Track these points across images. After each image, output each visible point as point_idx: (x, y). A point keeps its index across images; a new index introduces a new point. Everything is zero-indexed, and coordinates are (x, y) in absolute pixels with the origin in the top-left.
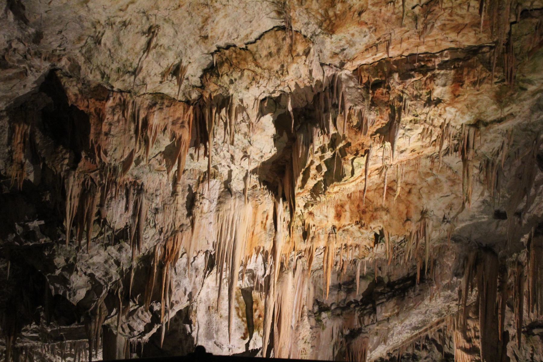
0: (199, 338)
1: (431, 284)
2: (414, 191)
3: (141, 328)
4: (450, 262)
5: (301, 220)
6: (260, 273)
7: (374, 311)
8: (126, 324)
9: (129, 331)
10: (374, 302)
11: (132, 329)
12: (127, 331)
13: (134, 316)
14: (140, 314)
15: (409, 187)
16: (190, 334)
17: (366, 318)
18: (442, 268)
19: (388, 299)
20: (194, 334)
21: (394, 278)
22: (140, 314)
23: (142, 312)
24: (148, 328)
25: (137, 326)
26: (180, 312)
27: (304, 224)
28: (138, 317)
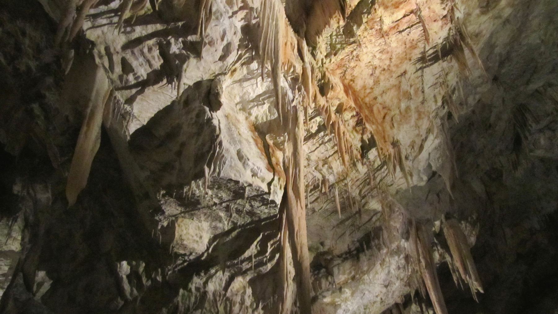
0: (222, 131)
1: (379, 249)
2: (388, 118)
3: (143, 72)
4: (397, 223)
5: (321, 72)
6: (290, 95)
7: (330, 273)
8: (120, 57)
9: (121, 73)
10: (326, 268)
11: (127, 67)
12: (118, 69)
13: (136, 50)
14: (146, 50)
15: (385, 111)
16: (210, 120)
17: (323, 281)
18: (390, 232)
19: (343, 261)
20: (215, 122)
21: (337, 252)
22: (146, 50)
23: (150, 50)
24: (155, 78)
25: (136, 66)
26: (198, 85)
27: (324, 76)
28: (142, 53)
